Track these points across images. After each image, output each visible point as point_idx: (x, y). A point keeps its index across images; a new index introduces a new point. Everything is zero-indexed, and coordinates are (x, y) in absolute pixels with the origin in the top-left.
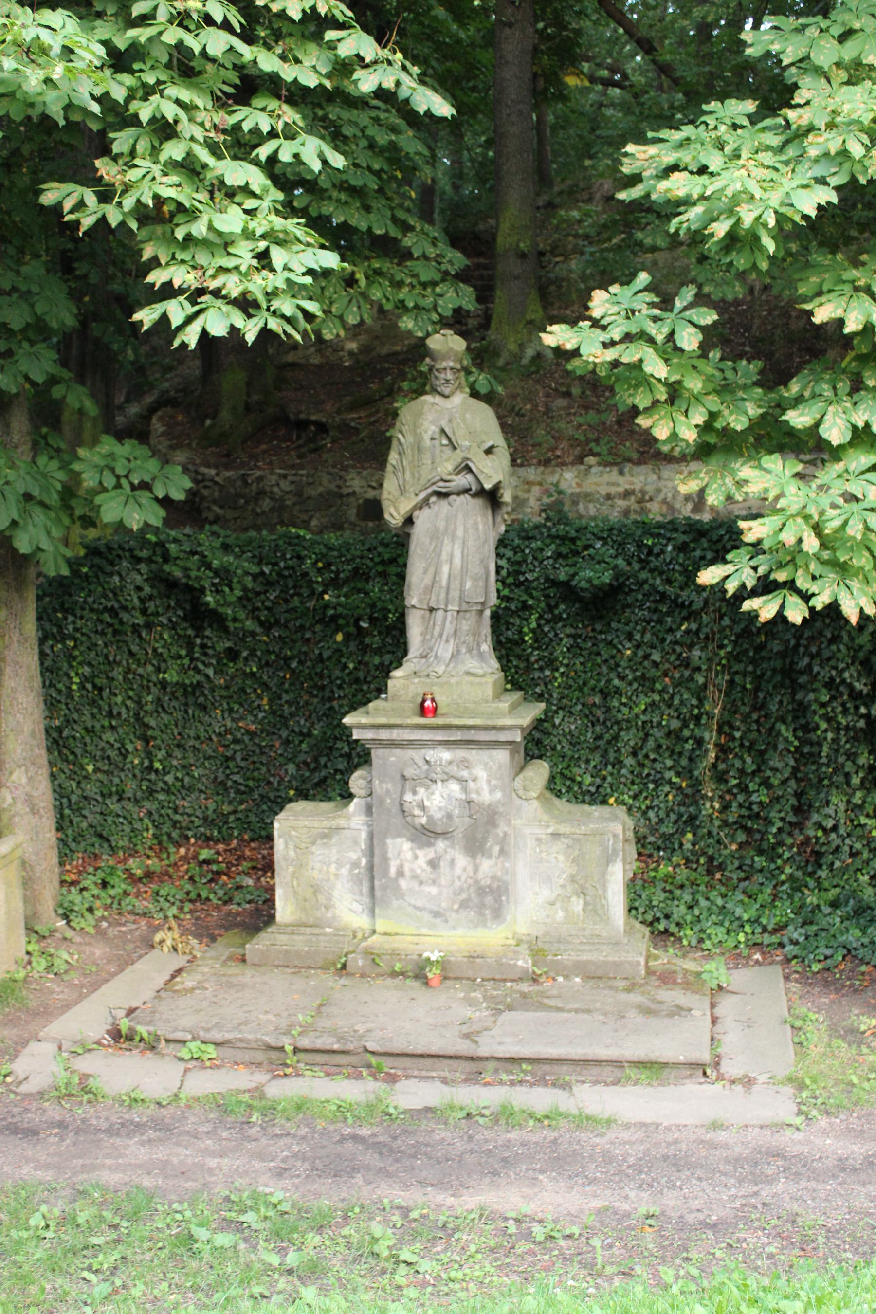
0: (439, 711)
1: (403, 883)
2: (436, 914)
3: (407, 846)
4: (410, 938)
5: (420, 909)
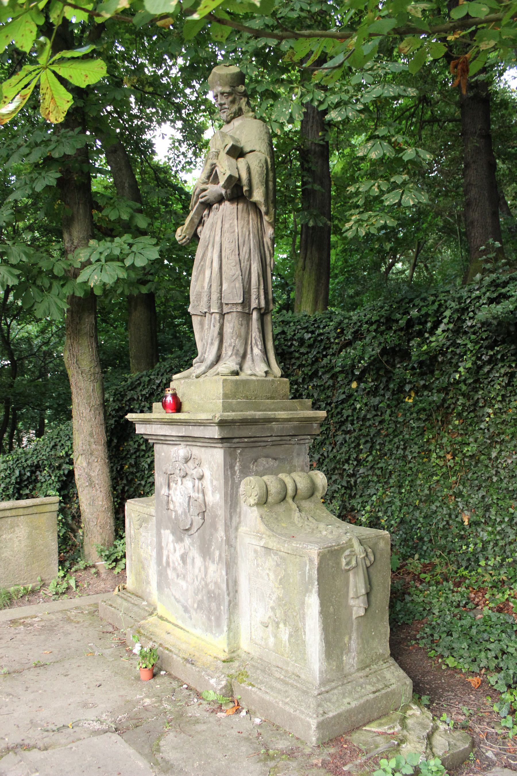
0: (185, 407)
3: (171, 538)
5: (178, 601)
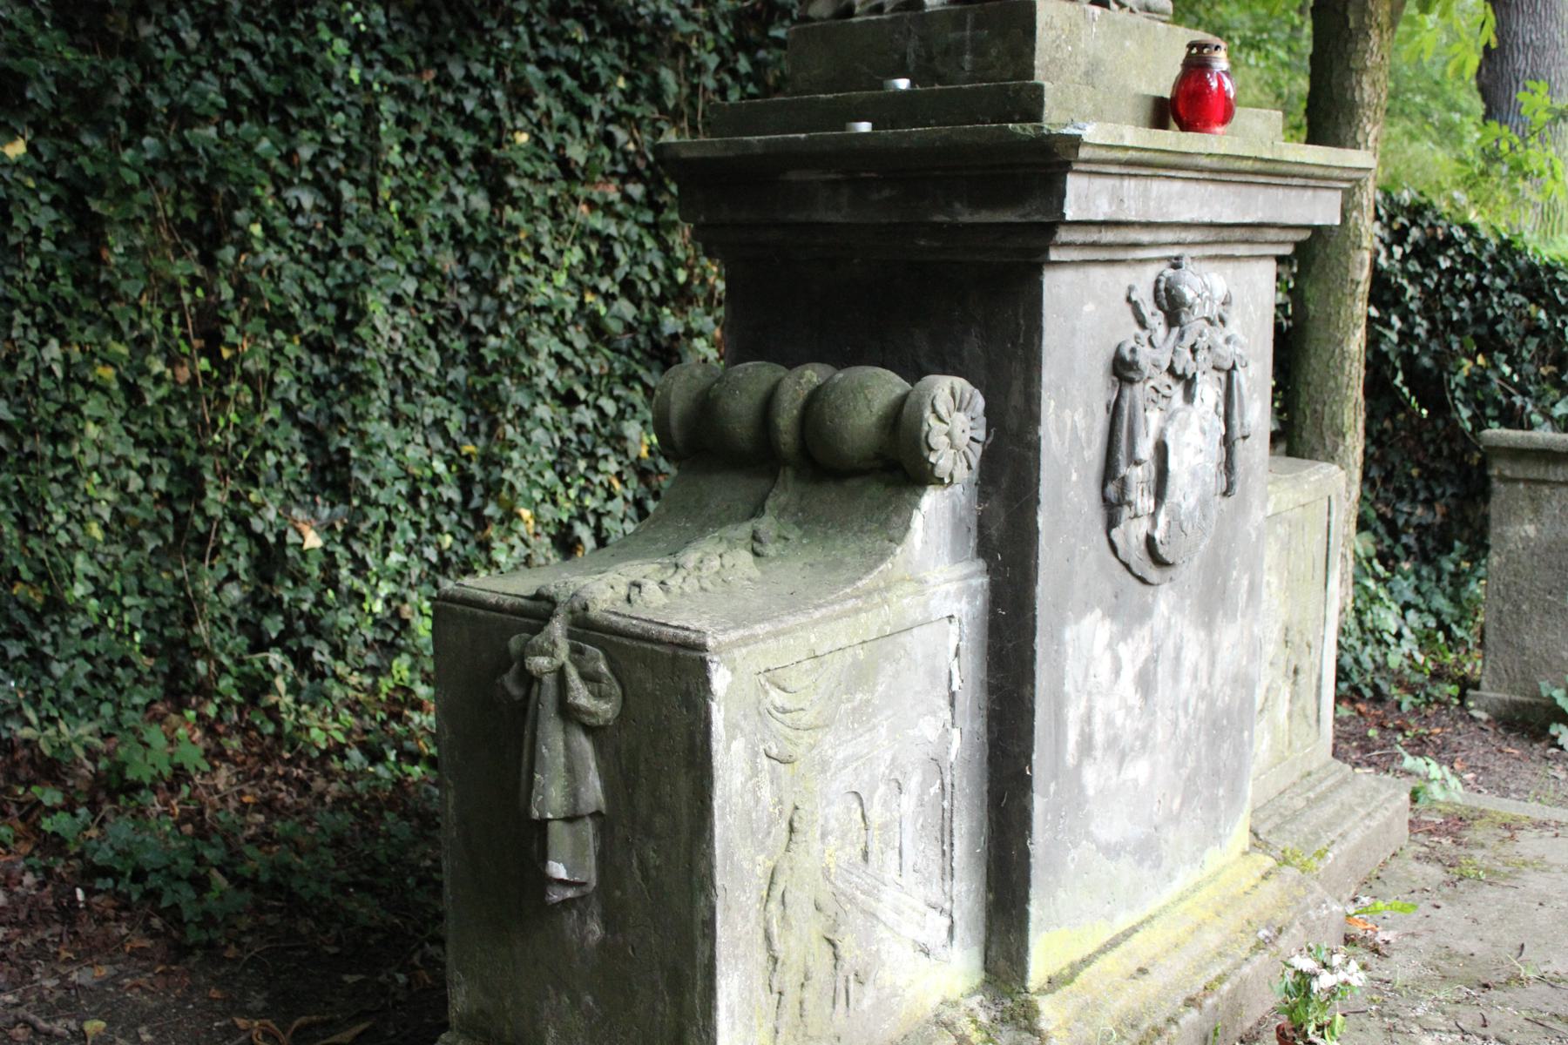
1: (1091, 777)
2: (1146, 850)
4: (1108, 962)
